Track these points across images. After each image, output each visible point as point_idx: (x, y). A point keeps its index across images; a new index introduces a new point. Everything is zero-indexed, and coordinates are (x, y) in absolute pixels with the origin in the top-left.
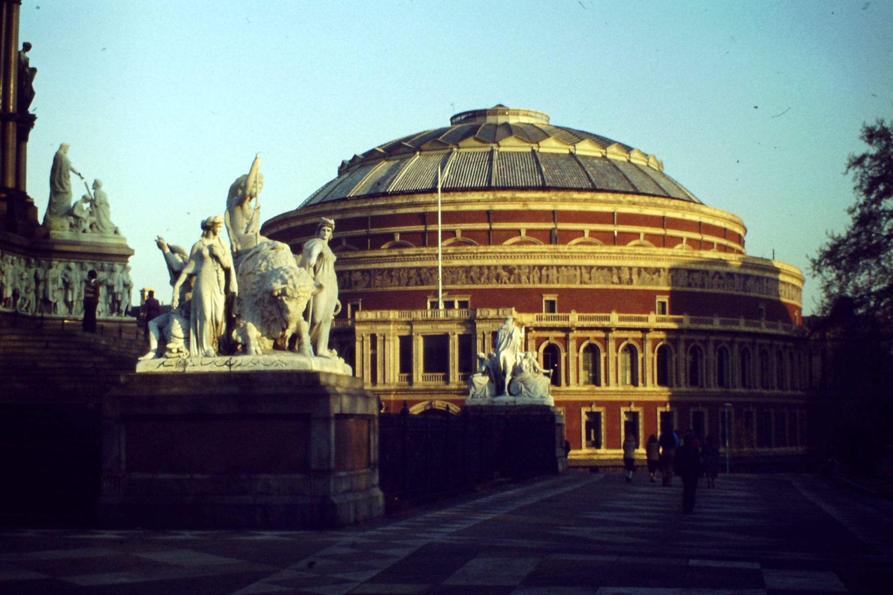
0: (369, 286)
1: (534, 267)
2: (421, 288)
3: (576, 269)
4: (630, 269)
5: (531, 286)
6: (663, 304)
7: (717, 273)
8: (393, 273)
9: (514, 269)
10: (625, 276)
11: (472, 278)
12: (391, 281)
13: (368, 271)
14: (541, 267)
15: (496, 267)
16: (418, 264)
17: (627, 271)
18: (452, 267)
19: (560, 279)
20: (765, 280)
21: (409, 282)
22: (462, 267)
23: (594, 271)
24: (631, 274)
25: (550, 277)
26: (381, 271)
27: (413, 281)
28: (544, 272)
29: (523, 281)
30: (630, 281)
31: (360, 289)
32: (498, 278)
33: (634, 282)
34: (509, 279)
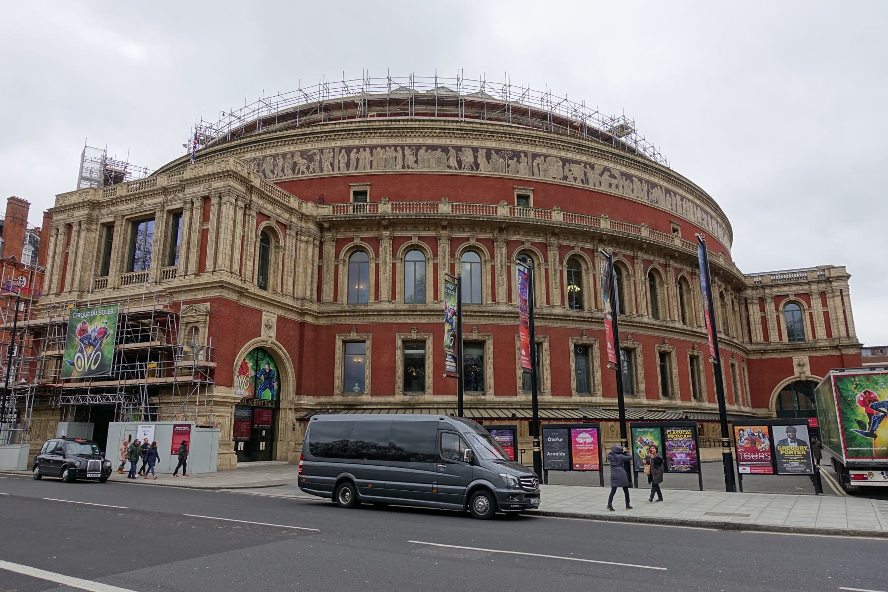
1: (341, 148)
4: (475, 150)
6: (527, 198)
7: (606, 169)
9: (315, 154)
10: (468, 158)
14: (349, 150)
15: (293, 154)
17: (471, 152)
20: (678, 198)
22: (255, 159)
23: (422, 151)
24: (476, 158)
25: (360, 163)
28: (353, 155)
29: (325, 168)
30: (477, 165)
32: (295, 164)
34: (308, 168)
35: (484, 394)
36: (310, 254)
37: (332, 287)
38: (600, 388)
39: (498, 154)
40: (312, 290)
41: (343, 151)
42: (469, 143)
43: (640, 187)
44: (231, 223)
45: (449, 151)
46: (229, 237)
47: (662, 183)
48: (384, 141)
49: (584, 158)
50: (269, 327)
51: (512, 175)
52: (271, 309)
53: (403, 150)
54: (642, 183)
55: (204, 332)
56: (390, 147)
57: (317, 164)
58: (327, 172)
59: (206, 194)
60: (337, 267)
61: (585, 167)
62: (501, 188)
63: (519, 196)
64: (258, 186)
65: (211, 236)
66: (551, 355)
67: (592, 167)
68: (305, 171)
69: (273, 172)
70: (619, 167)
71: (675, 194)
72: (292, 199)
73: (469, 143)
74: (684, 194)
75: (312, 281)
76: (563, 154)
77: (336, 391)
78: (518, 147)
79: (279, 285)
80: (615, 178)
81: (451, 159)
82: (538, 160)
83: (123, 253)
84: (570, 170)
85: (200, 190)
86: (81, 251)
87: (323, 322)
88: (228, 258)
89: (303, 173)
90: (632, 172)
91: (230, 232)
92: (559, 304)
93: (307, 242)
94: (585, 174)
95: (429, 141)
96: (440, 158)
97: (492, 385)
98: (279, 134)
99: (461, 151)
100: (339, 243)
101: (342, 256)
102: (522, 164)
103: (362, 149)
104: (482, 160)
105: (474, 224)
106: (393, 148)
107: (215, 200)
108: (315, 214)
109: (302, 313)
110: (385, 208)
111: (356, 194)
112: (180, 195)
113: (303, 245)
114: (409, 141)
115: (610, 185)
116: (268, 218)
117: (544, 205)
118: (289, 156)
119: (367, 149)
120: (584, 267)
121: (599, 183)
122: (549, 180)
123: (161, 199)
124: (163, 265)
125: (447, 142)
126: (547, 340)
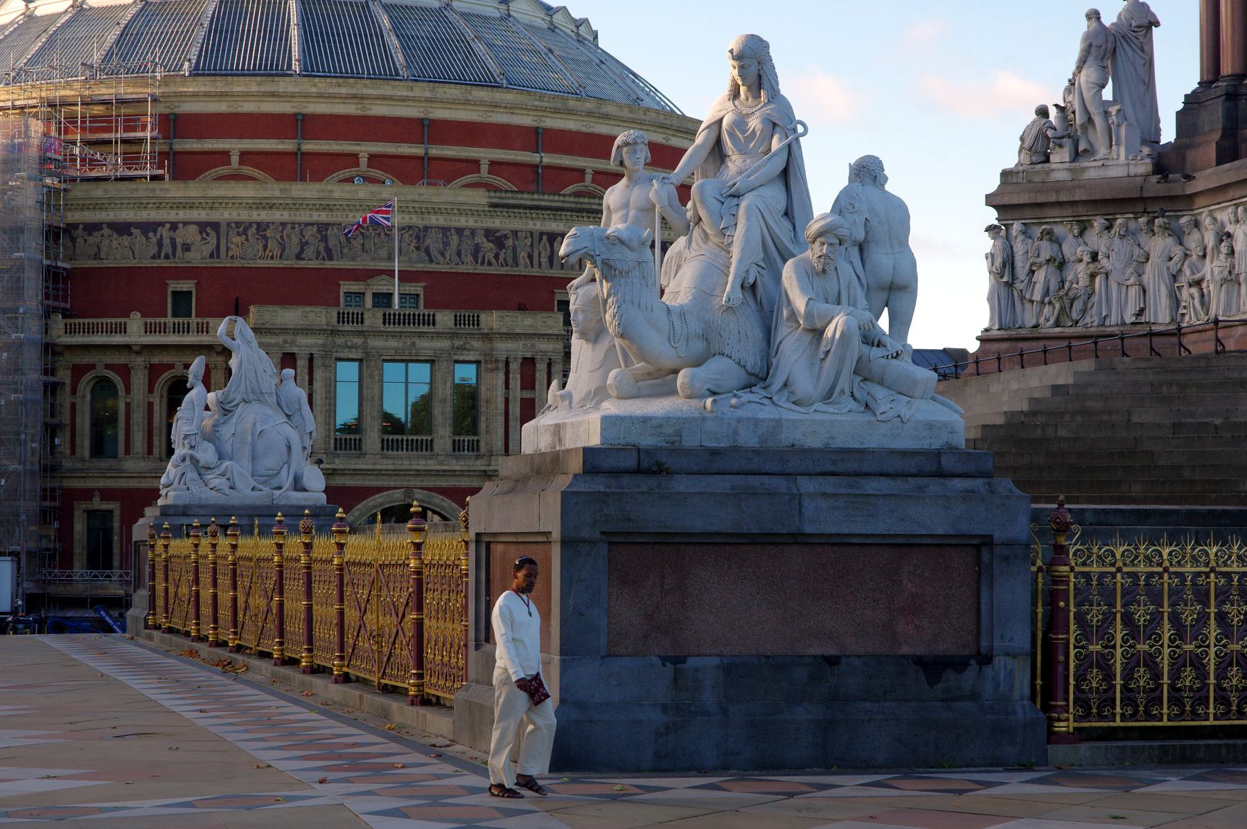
0: (212, 256)
1: (542, 234)
2: (329, 264)
5: (535, 271)
8: (269, 233)
9: (506, 236)
11: (427, 251)
12: (265, 247)
13: (215, 226)
15: (473, 232)
16: (323, 217)
21: (302, 250)
22: (410, 227)
26: (242, 228)
27: (309, 252)
29: (522, 261)
31: (197, 257)
32: (477, 250)
34: (497, 257)
41: (545, 238)
57: (510, 253)
58: (523, 269)
59: (529, 355)
68: (493, 260)
69: (442, 254)
85: (518, 349)
112: (477, 344)
118: (467, 233)
123: (445, 344)
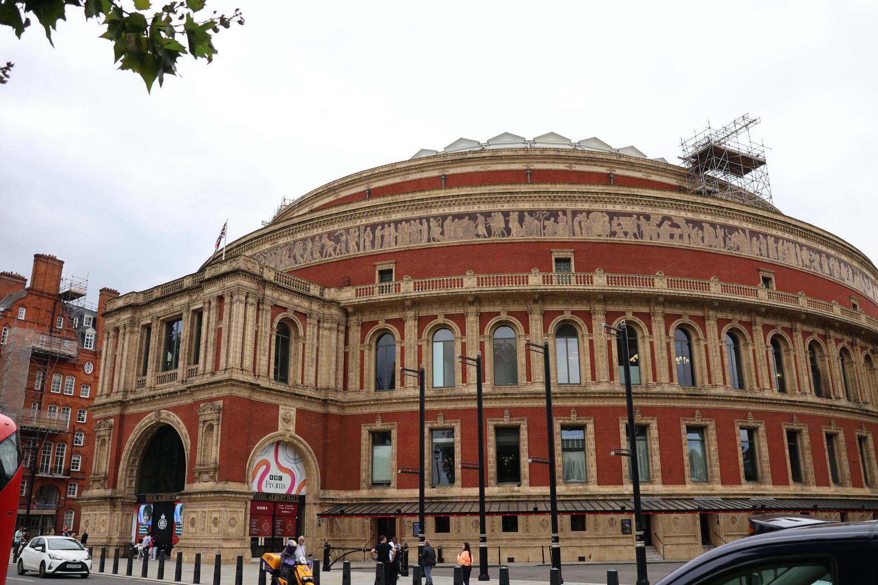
1: (366, 226)
3: (421, 224)
4: (506, 214)
6: (568, 260)
7: (665, 218)
9: (341, 235)
10: (498, 223)
14: (374, 227)
15: (321, 236)
17: (502, 217)
18: (277, 248)
19: (399, 240)
20: (771, 240)
22: (286, 244)
23: (448, 221)
24: (507, 222)
25: (386, 240)
28: (378, 233)
30: (508, 231)
33: (514, 232)
34: (335, 250)
35: (519, 486)
36: (334, 341)
37: (358, 374)
38: (660, 474)
39: (532, 216)
40: (336, 379)
41: (369, 229)
42: (499, 207)
43: (713, 234)
44: (241, 321)
45: (477, 218)
46: (240, 335)
47: (744, 225)
48: (409, 215)
49: (637, 209)
50: (287, 421)
51: (548, 238)
52: (289, 402)
53: (428, 222)
54: (715, 228)
55: (217, 430)
56: (415, 220)
57: (344, 245)
58: (353, 252)
59: (220, 293)
60: (362, 352)
61: (638, 219)
62: (536, 255)
63: (557, 260)
64: (272, 279)
65: (224, 334)
66: (597, 439)
67: (647, 217)
68: (333, 253)
69: (302, 257)
70: (683, 214)
71: (766, 236)
72: (312, 287)
73: (499, 207)
74: (780, 234)
75: (337, 370)
76: (610, 207)
77: (363, 485)
78: (556, 206)
79: (300, 376)
80: (678, 226)
81: (480, 227)
82: (579, 217)
83: (158, 353)
84: (619, 225)
86: (125, 353)
87: (350, 411)
88: (239, 355)
89: (330, 255)
90: (702, 217)
91: (240, 330)
92: (606, 379)
93: (330, 329)
94: (639, 226)
95: (456, 210)
96: (467, 227)
97: (528, 475)
98: (308, 217)
99: (490, 216)
100: (365, 327)
101: (367, 341)
102: (560, 224)
103: (386, 226)
104: (514, 225)
105: (504, 297)
106: (418, 221)
107: (227, 300)
108: (339, 298)
109: (325, 402)
110: (407, 288)
111: (381, 272)
113: (326, 333)
114: (434, 212)
115: (672, 236)
116: (285, 309)
117: (586, 267)
118: (317, 238)
119: (392, 224)
120: (639, 335)
121: (656, 236)
122: (594, 238)
123: (185, 300)
124: (189, 364)
125: (475, 208)
126: (592, 421)
